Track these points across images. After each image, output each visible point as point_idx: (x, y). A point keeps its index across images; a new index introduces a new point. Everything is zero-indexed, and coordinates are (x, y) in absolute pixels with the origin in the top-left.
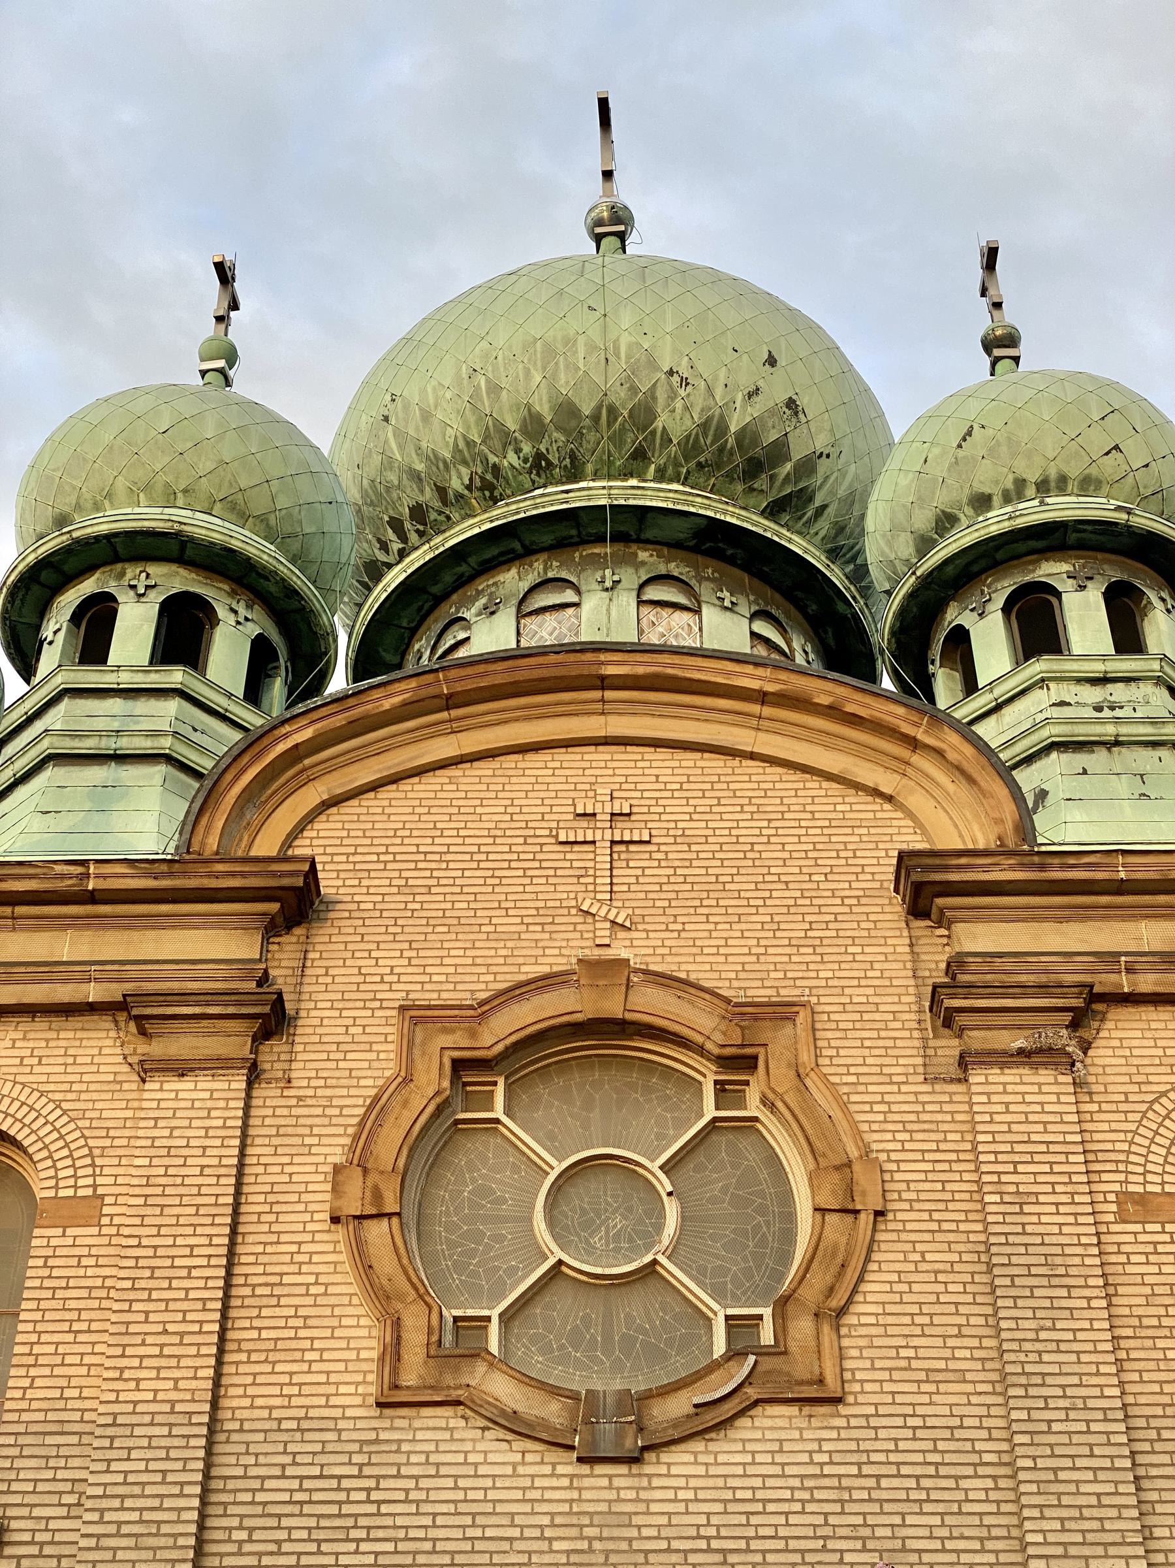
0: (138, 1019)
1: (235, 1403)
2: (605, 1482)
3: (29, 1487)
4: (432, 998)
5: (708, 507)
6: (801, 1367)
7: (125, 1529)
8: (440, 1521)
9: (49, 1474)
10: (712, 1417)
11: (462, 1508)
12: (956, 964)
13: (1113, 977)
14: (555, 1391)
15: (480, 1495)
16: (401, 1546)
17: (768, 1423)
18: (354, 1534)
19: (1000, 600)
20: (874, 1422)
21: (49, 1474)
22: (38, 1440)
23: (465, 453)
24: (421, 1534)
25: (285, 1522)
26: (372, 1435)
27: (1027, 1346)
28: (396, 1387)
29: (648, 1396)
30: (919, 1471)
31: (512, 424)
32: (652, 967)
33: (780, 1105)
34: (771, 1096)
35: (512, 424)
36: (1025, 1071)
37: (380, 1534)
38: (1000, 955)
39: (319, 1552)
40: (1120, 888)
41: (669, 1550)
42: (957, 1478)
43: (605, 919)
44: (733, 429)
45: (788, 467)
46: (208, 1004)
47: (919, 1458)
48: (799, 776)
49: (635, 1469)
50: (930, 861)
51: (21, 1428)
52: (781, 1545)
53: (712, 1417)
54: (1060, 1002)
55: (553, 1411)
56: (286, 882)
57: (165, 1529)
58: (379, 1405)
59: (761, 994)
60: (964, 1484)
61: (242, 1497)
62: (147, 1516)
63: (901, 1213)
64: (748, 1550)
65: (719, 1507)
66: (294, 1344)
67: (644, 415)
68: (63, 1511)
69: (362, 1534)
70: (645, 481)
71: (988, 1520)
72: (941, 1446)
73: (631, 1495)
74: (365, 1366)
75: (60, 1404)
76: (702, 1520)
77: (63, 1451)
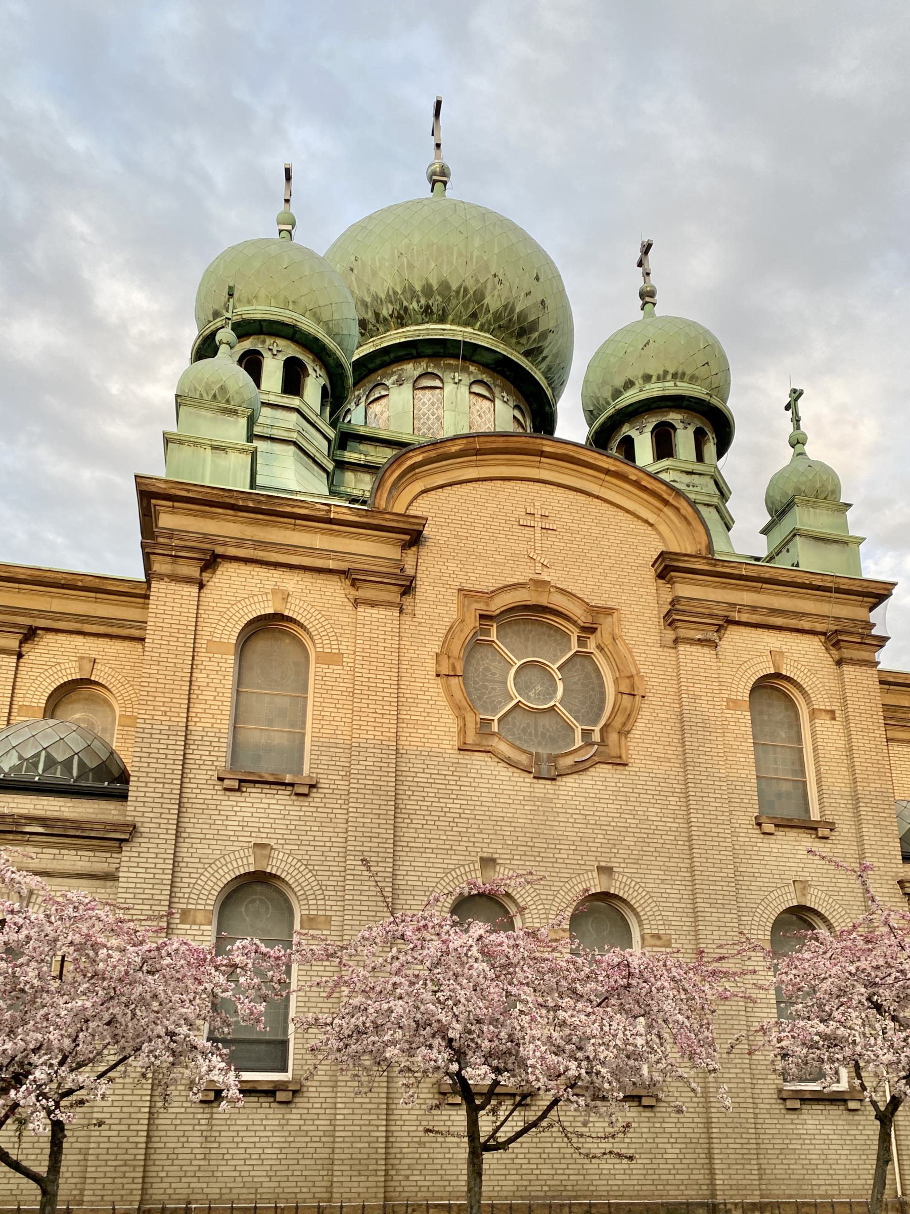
1: (403, 743)
2: (543, 786)
3: (326, 767)
5: (505, 350)
6: (614, 751)
7: (368, 787)
8: (483, 794)
9: (333, 763)
10: (582, 766)
11: (491, 790)
12: (675, 601)
14: (524, 752)
15: (497, 787)
16: (470, 802)
17: (601, 770)
18: (452, 796)
19: (650, 427)
20: (638, 774)
21: (333, 763)
22: (327, 749)
24: (476, 799)
25: (426, 790)
26: (456, 761)
27: (695, 752)
29: (558, 756)
30: (653, 792)
33: (606, 649)
34: (602, 645)
37: (462, 797)
39: (439, 802)
41: (566, 813)
42: (667, 796)
43: (539, 562)
45: (536, 335)
46: (384, 577)
47: (653, 788)
48: (615, 509)
49: (554, 782)
51: (320, 744)
52: (605, 814)
53: (582, 766)
55: (523, 759)
57: (383, 788)
58: (459, 749)
60: (669, 798)
61: (409, 779)
62: (375, 783)
63: (650, 697)
64: (594, 815)
65: (583, 799)
66: (425, 723)
68: (340, 778)
69: (455, 797)
71: (676, 812)
72: (662, 784)
73: (552, 792)
74: (452, 734)
75: (335, 736)
76: (578, 803)
77: (338, 755)
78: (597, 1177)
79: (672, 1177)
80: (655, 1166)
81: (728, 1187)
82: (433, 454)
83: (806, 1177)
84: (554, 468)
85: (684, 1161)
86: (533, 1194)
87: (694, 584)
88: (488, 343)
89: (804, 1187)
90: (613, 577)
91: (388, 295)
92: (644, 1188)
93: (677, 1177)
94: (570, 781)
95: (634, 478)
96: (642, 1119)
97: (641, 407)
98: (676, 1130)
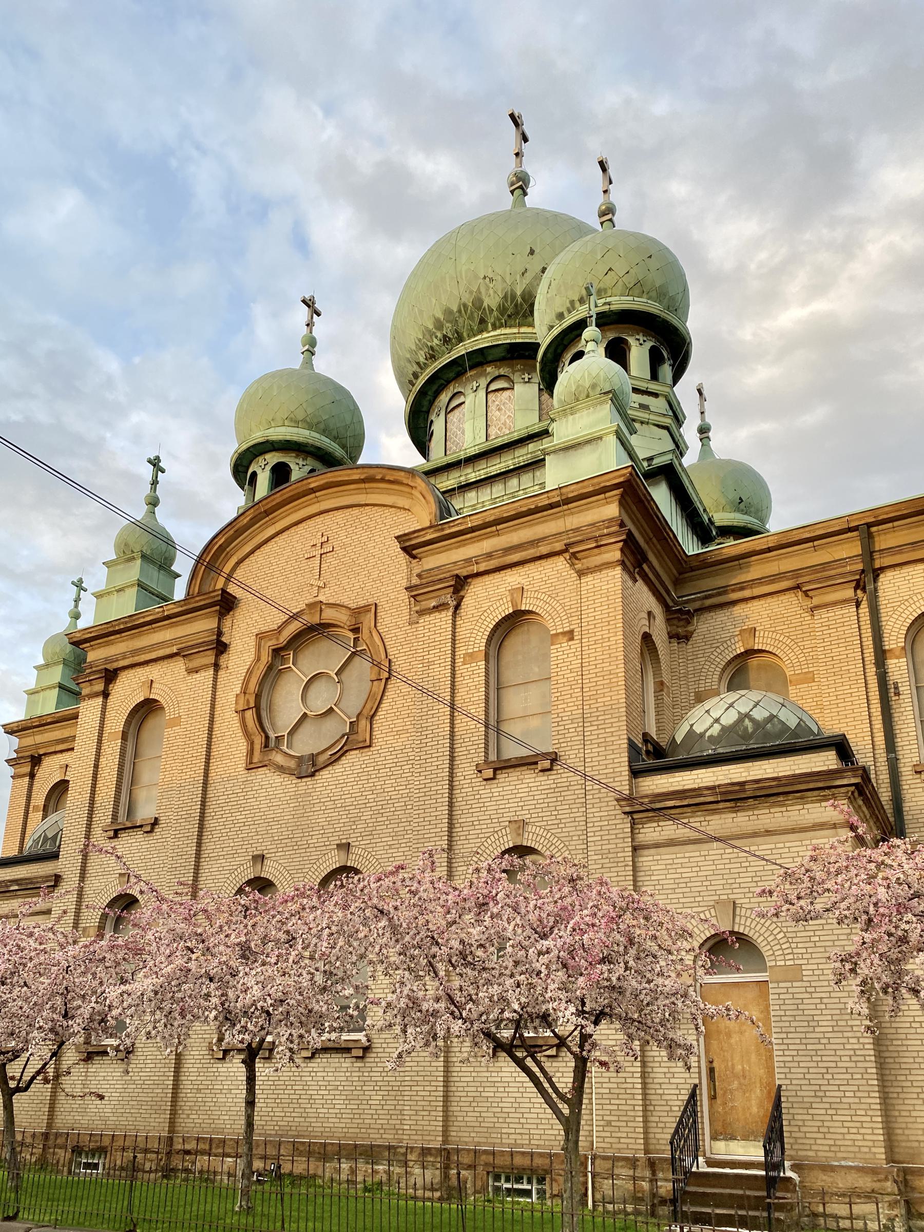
0: (184, 656)
4: (266, 629)
10: (334, 758)
13: (471, 568)
23: (420, 345)
28: (251, 763)
31: (431, 327)
32: (330, 602)
35: (431, 327)
36: (437, 614)
38: (433, 569)
40: (473, 530)
44: (519, 293)
50: (405, 538)
54: (446, 584)
55: (292, 764)
56: (216, 599)
59: (362, 603)
67: (478, 303)
70: (489, 332)
78: (314, 1120)
79: (374, 1121)
80: (361, 1111)
81: (414, 1132)
82: (231, 532)
83: (497, 1125)
84: (339, 494)
85: (385, 1107)
86: (268, 1132)
87: (438, 553)
88: (488, 342)
89: (493, 1135)
90: (375, 575)
91: (417, 345)
92: (350, 1130)
93: (378, 1122)
94: (325, 774)
95: (379, 477)
96: (354, 1069)
97: (555, 350)
98: (381, 1079)
